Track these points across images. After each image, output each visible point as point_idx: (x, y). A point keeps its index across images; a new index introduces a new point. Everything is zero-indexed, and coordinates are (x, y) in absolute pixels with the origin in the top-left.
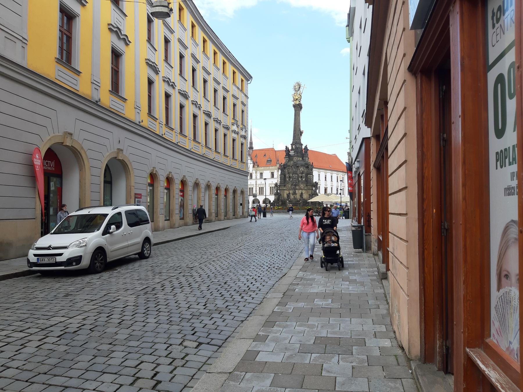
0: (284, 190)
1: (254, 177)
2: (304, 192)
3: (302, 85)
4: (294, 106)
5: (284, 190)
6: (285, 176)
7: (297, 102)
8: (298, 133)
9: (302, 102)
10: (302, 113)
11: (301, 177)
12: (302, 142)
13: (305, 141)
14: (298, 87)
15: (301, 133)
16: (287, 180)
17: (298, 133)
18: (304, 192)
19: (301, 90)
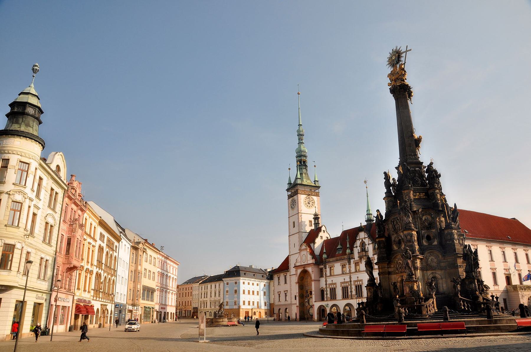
2: (439, 274)
3: (403, 49)
4: (393, 91)
6: (389, 239)
8: (409, 143)
9: (407, 82)
10: (415, 106)
11: (428, 238)
12: (421, 160)
13: (425, 156)
14: (396, 58)
15: (418, 142)
16: (395, 247)
17: (409, 143)
18: (439, 274)
19: (403, 59)
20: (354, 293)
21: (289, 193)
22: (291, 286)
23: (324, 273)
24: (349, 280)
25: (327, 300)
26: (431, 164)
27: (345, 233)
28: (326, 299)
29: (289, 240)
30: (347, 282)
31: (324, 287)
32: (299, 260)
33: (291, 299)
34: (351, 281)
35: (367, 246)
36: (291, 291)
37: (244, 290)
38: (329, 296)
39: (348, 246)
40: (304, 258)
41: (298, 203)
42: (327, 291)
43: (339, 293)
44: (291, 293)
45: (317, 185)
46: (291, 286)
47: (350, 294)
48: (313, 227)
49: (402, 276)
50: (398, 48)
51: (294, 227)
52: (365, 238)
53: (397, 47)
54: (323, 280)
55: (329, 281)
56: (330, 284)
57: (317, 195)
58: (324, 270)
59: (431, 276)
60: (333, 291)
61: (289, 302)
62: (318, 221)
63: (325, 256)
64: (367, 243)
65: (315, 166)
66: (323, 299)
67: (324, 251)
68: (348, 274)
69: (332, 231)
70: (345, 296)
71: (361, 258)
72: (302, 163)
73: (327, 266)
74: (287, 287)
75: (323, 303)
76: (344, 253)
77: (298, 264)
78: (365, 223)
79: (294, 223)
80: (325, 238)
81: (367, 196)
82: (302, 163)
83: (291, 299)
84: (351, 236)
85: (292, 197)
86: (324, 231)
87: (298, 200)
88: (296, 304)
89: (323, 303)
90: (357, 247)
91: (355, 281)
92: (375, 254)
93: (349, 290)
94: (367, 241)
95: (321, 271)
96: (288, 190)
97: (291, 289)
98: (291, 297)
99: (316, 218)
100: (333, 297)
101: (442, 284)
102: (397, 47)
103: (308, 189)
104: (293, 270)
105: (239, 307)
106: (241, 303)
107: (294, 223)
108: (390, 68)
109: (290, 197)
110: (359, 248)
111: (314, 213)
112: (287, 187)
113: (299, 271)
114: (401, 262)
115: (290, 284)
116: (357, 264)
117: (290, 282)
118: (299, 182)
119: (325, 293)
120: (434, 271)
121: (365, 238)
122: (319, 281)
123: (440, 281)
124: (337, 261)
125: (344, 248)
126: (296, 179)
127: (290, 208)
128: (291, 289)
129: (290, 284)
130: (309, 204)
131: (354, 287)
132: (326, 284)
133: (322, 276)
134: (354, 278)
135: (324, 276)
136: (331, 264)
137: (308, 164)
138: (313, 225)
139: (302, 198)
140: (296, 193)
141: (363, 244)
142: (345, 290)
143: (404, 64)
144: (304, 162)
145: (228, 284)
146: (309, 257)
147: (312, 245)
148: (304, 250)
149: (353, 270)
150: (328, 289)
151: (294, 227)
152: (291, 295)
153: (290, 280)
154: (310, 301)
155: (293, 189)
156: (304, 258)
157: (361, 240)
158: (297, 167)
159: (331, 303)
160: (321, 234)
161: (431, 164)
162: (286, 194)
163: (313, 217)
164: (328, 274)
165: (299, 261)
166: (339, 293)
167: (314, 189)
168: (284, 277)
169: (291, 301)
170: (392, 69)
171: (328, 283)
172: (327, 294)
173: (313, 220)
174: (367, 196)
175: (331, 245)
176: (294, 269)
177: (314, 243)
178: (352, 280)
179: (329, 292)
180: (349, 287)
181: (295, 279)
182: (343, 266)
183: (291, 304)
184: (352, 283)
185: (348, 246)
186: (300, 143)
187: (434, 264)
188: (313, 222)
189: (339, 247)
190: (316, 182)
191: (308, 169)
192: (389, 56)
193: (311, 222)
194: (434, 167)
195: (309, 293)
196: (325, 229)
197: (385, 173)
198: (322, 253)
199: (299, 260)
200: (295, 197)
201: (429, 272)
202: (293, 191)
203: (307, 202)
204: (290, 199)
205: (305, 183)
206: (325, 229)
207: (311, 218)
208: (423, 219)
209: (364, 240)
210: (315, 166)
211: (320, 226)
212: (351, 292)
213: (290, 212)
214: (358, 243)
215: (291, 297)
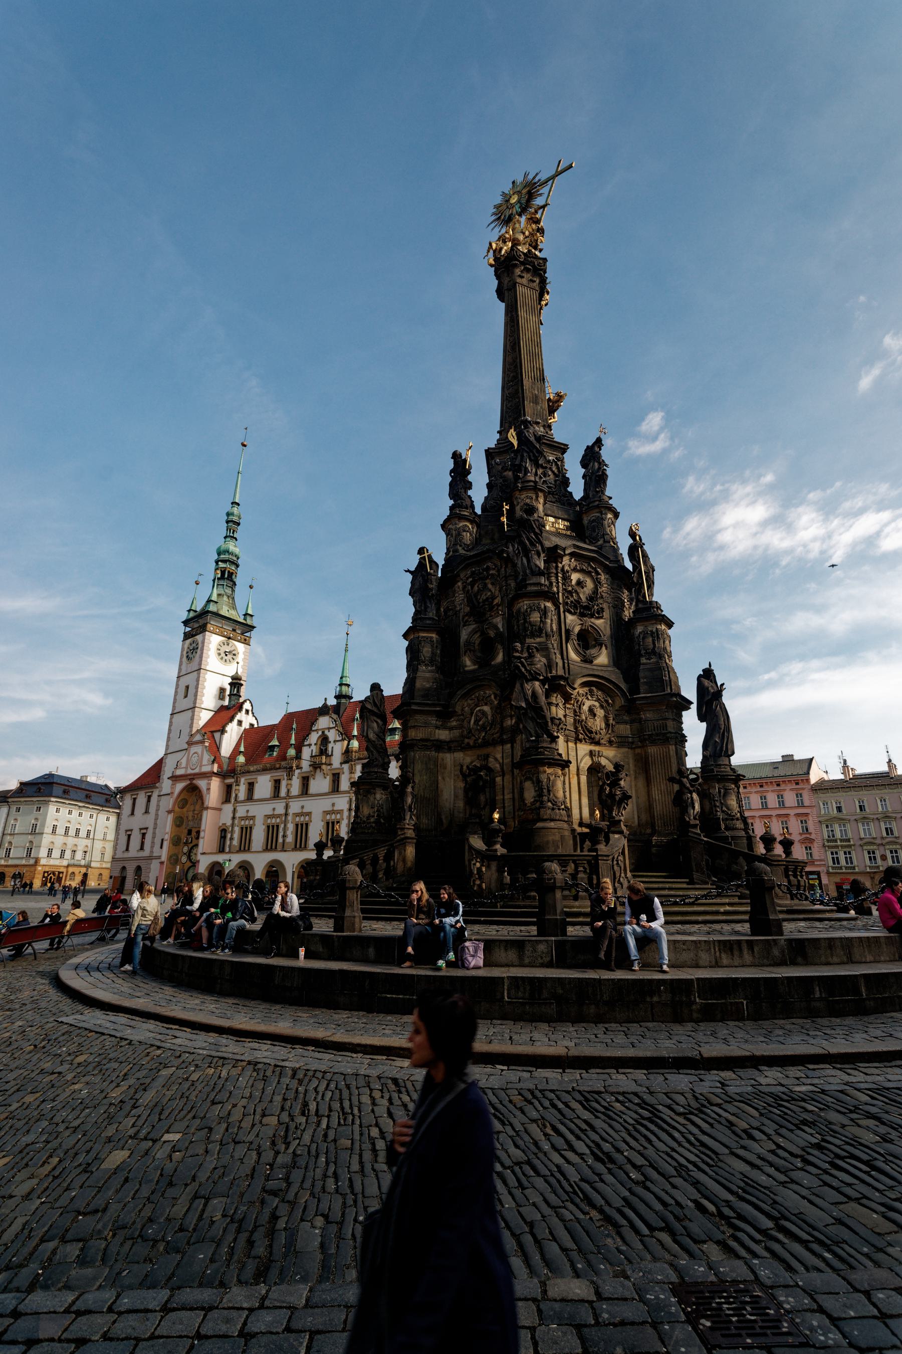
0: (440, 746)
5: (440, 746)
16: (469, 664)
20: (290, 839)
21: (188, 629)
22: (156, 819)
23: (233, 795)
24: (283, 811)
25: (230, 852)
26: (599, 442)
27: (289, 718)
28: (227, 850)
29: (171, 723)
30: (279, 816)
31: (229, 823)
32: (184, 762)
33: (152, 847)
34: (286, 814)
35: (330, 746)
36: (155, 828)
37: (55, 827)
38: (236, 842)
39: (293, 741)
40: (195, 759)
41: (202, 650)
42: (232, 832)
43: (259, 836)
44: (154, 833)
45: (249, 622)
46: (156, 819)
47: (280, 840)
48: (226, 703)
49: (487, 757)
50: (530, 177)
51: (186, 696)
52: (329, 729)
54: (228, 808)
55: (241, 811)
56: (242, 818)
57: (246, 642)
58: (234, 788)
60: (246, 832)
61: (146, 853)
62: (238, 691)
63: (241, 759)
64: (331, 739)
65: (251, 587)
66: (221, 850)
67: (242, 749)
68: (284, 798)
69: (264, 711)
70: (271, 844)
71: (316, 766)
72: (226, 574)
73: (242, 780)
74: (149, 821)
75: (220, 858)
76: (283, 757)
77: (179, 772)
78: (332, 702)
79: (187, 687)
80: (246, 725)
81: (346, 651)
82: (226, 574)
83: (152, 847)
84: (301, 722)
85: (193, 636)
86: (247, 712)
87: (203, 642)
88: (159, 857)
89: (220, 858)
90: (310, 745)
91: (297, 815)
92: (345, 762)
93: (281, 834)
95: (229, 788)
96: (186, 623)
97: (156, 824)
98: (153, 843)
99: (236, 683)
100: (245, 846)
102: (526, 175)
103: (228, 627)
104: (166, 785)
105: (37, 860)
106: (43, 853)
107: (187, 687)
108: (497, 229)
109: (187, 636)
110: (313, 747)
111: (233, 673)
112: (184, 616)
113: (180, 786)
114: (486, 708)
115: (157, 815)
117: (157, 810)
118: (212, 608)
119: (229, 836)
121: (329, 729)
122: (220, 810)
124: (265, 770)
125: (284, 744)
126: (209, 601)
127: (185, 659)
128: (156, 824)
129: (157, 815)
130: (228, 655)
131: (291, 827)
132: (234, 818)
133: (227, 800)
134: (295, 807)
135: (233, 800)
136: (250, 777)
137: (237, 580)
138: (227, 699)
139: (213, 641)
140: (203, 629)
141: (324, 740)
142: (272, 831)
144: (231, 574)
145: (18, 810)
146: (207, 757)
147: (217, 735)
148: (197, 743)
149: (296, 788)
150: (237, 830)
151: (186, 696)
152: (154, 838)
153: (158, 806)
154: (194, 851)
155: (197, 624)
156: (195, 759)
157: (320, 733)
158: (214, 581)
159: (237, 858)
160: (239, 716)
161: (599, 442)
162: (182, 629)
163: (230, 680)
164: (242, 795)
165: (184, 765)
166: (259, 836)
167: (242, 629)
168: (145, 800)
169: (152, 852)
171: (238, 815)
172: (231, 839)
173: (228, 688)
174: (346, 651)
175: (257, 742)
176: (170, 782)
177: (223, 731)
178: (291, 811)
179: (236, 836)
180: (282, 826)
181: (168, 803)
182: (277, 783)
183: (150, 858)
184: (290, 818)
185: (293, 741)
186: (230, 536)
187: (598, 724)
188: (228, 692)
189: (275, 742)
190: (248, 618)
191: (237, 589)
192: (499, 200)
193: (222, 690)
194: (605, 454)
195: (194, 834)
196: (250, 708)
197: (456, 456)
198: (236, 752)
199: (184, 762)
200: (199, 638)
202: (196, 625)
203: (222, 652)
204: (188, 642)
205: (224, 611)
206: (250, 708)
207: (226, 683)
209: (326, 732)
210: (251, 587)
211: (241, 700)
212: (284, 836)
213: (184, 667)
214: (314, 738)
215: (153, 843)
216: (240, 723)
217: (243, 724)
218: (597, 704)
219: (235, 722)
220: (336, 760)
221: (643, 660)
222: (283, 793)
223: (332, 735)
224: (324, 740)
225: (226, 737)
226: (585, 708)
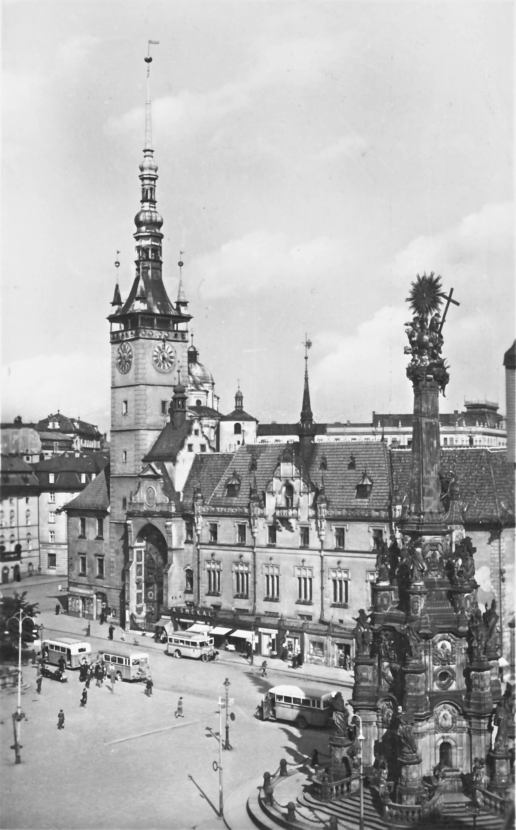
1: (314, 542)
4: (413, 373)
7: (426, 360)
35: (296, 497)
53: (432, 275)
59: (441, 741)
94: (298, 484)
101: (457, 755)
102: (432, 275)
108: (412, 310)
116: (273, 530)
120: (446, 734)
123: (454, 750)
141: (290, 489)
143: (442, 324)
170: (416, 315)
177: (174, 461)
182: (242, 529)
201: (439, 735)
207: (168, 395)
208: (439, 645)
209: (291, 482)
216: (190, 446)
217: (194, 448)
218: (448, 713)
219: (186, 447)
220: (305, 513)
221: (473, 689)
222: (248, 541)
223: (298, 484)
224: (290, 489)
225: (179, 466)
226: (442, 715)
